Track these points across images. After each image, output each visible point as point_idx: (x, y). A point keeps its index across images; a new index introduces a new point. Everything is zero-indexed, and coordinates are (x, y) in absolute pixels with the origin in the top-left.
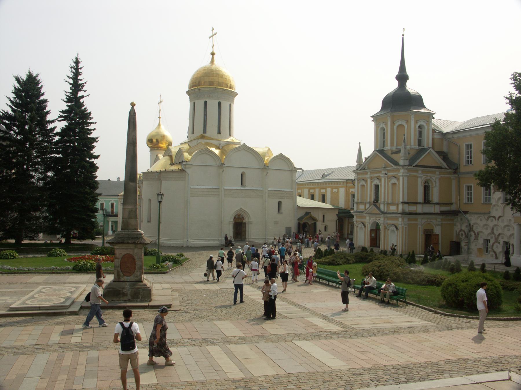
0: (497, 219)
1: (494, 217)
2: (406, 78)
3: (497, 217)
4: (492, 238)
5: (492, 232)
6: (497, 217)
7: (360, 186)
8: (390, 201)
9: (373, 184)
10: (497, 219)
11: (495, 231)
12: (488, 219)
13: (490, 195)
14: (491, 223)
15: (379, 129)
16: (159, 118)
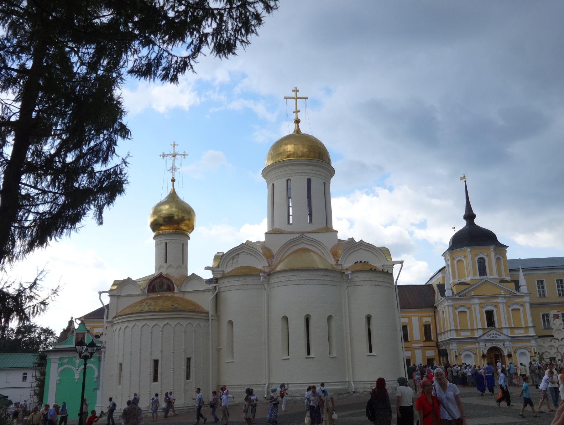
0: (560, 340)
1: (557, 339)
2: (474, 216)
3: (560, 339)
4: (558, 356)
5: (558, 352)
6: (560, 339)
7: (511, 311)
8: (513, 326)
9: (484, 310)
10: (560, 340)
11: (559, 350)
12: (551, 341)
13: (548, 321)
14: (557, 344)
15: (476, 259)
16: (173, 180)
